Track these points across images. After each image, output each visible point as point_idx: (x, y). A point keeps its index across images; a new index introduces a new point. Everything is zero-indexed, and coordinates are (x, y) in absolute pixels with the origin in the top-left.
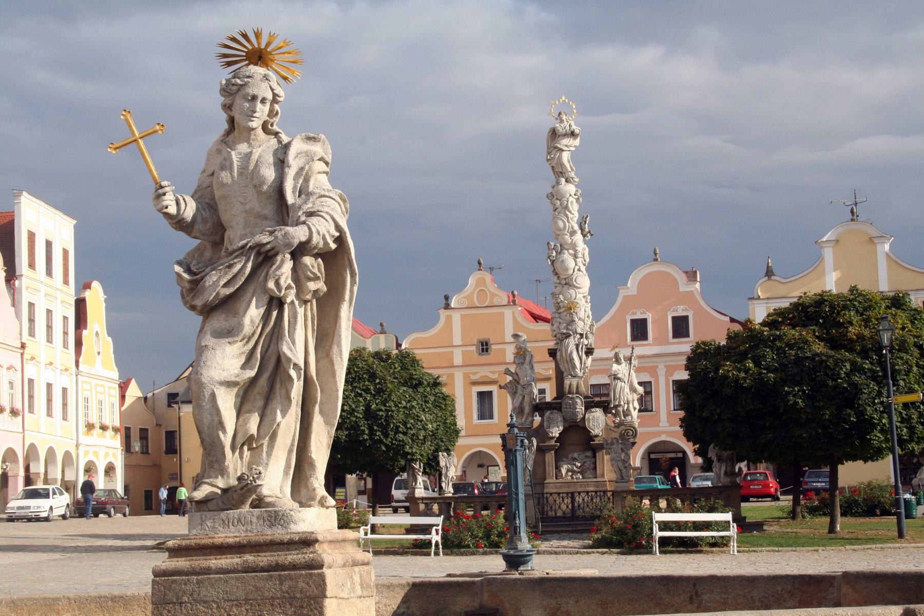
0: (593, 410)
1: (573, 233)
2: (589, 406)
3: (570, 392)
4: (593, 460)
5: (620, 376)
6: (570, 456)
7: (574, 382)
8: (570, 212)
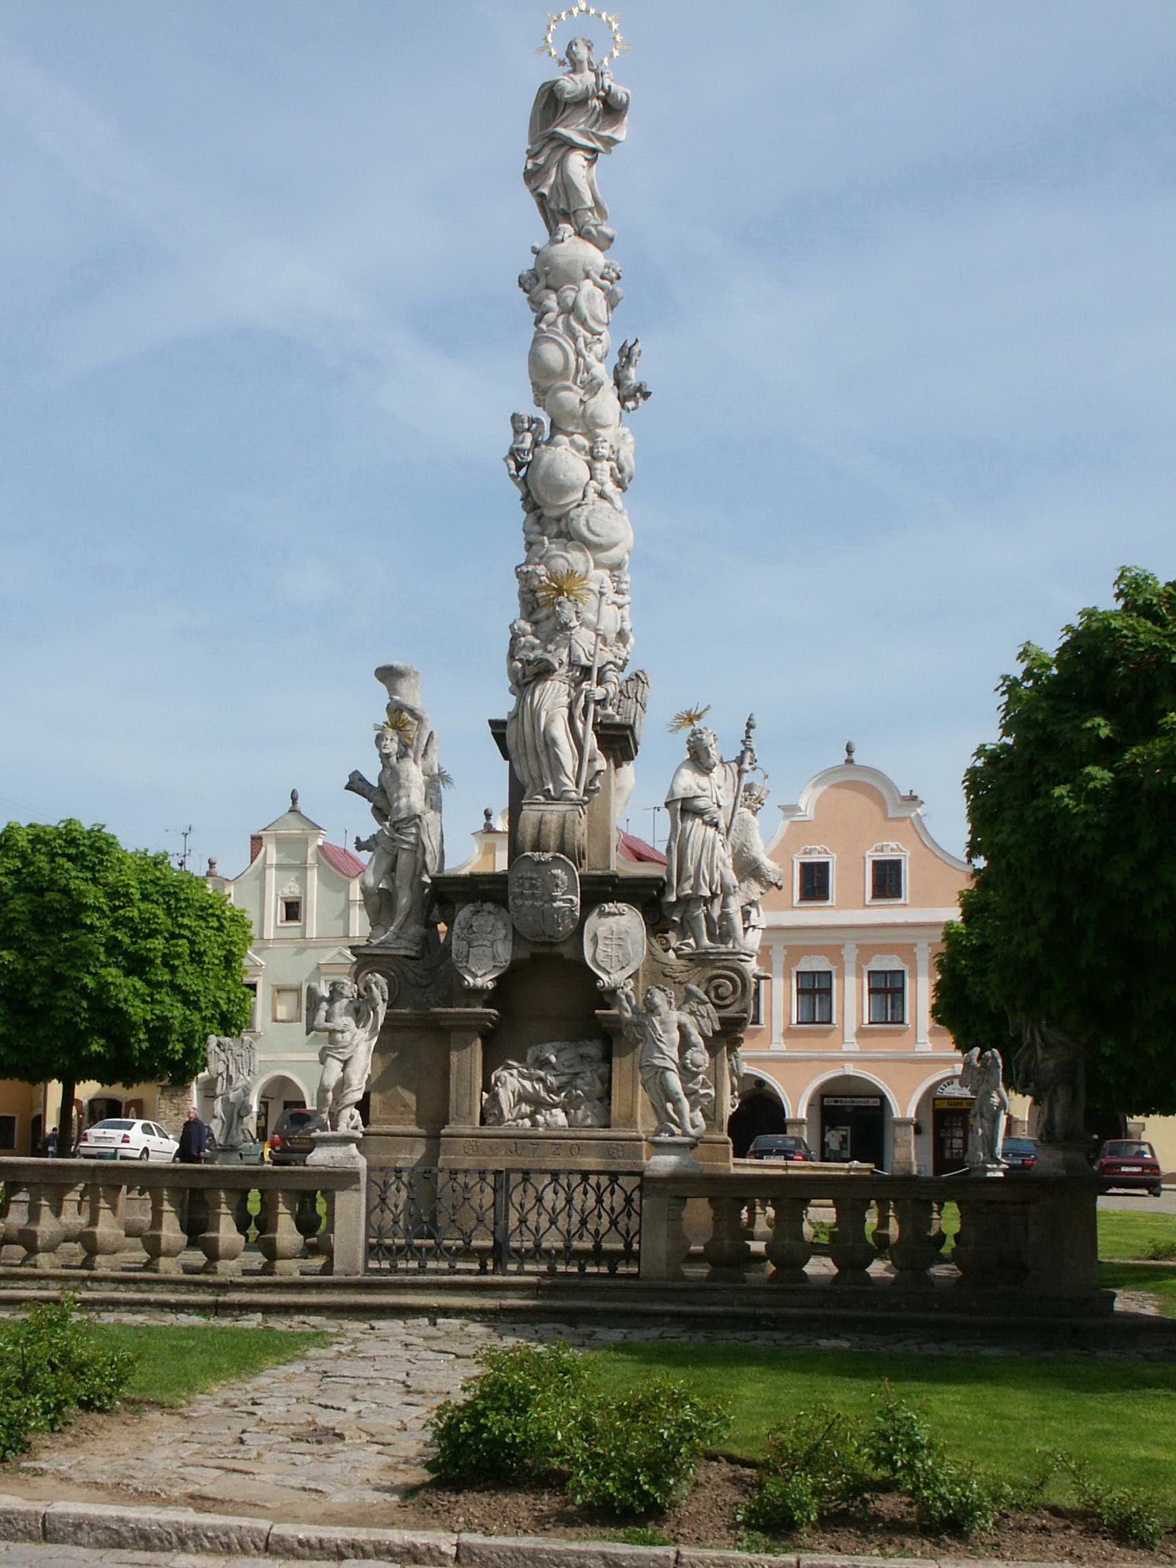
0: (609, 907)
1: (592, 387)
2: (600, 891)
3: (536, 847)
4: (603, 1069)
5: (701, 803)
6: (531, 1053)
7: (553, 813)
8: (583, 322)
